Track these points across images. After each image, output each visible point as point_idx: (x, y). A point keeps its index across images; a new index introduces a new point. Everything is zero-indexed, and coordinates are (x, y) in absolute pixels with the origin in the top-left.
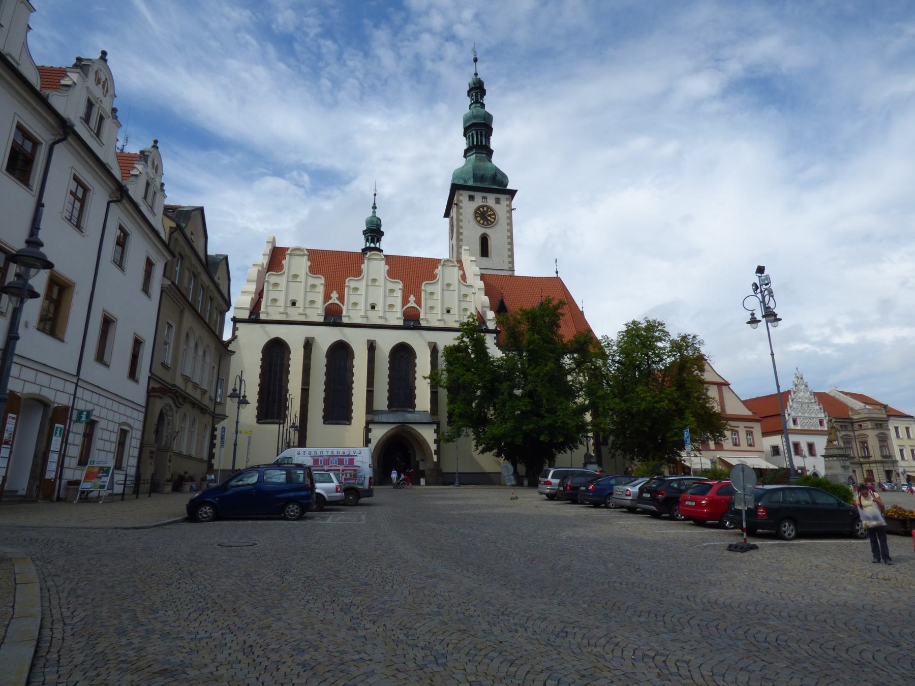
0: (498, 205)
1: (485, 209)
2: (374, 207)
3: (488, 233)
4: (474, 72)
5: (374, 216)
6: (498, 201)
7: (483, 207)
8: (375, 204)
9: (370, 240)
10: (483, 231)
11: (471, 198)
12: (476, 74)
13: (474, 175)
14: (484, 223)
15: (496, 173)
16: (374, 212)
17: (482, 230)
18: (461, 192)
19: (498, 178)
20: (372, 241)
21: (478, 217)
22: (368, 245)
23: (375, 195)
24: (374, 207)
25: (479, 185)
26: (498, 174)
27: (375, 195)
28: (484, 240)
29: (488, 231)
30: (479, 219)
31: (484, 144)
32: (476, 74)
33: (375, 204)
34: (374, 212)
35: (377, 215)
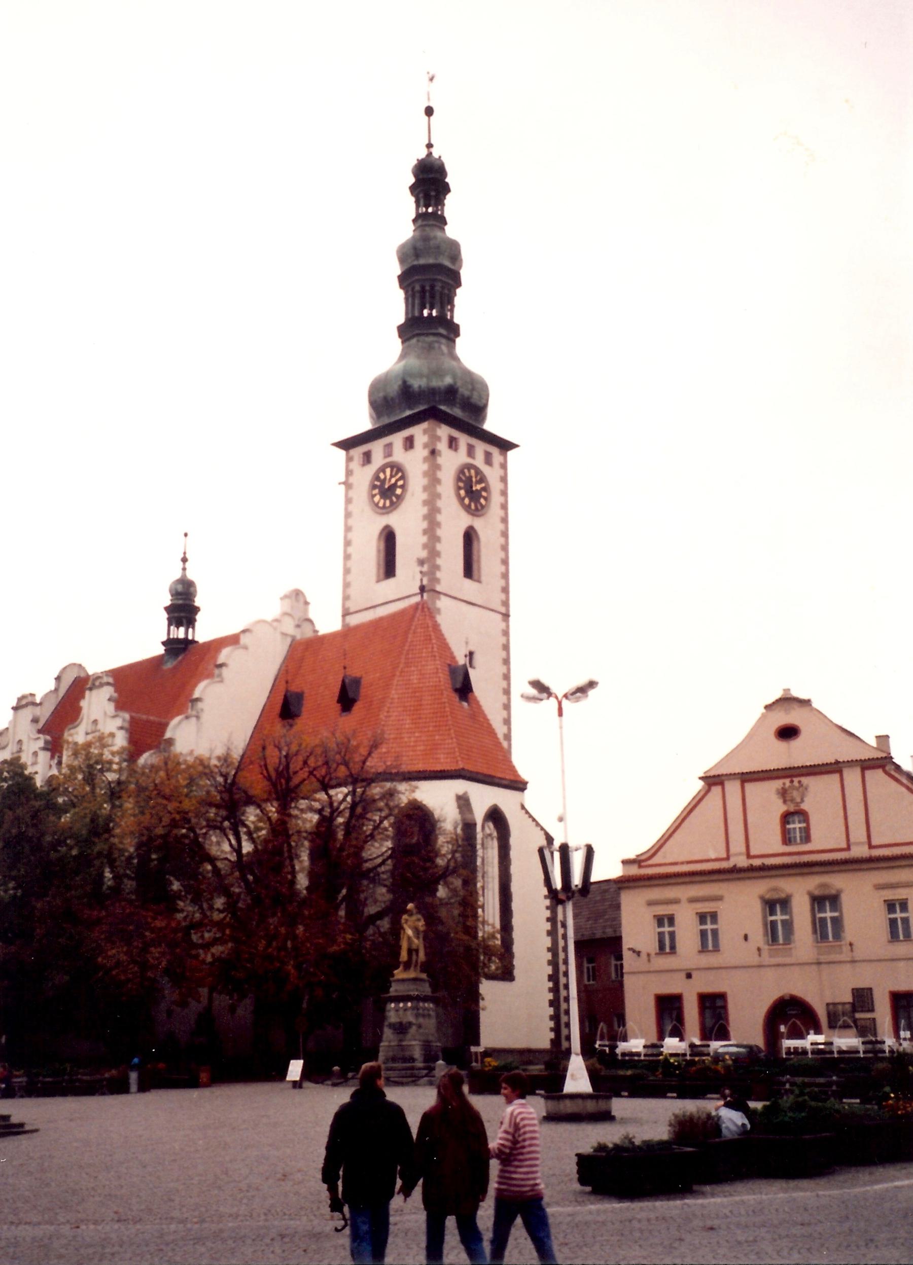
0: (411, 453)
4: (427, 142)
5: (184, 576)
6: (409, 443)
7: (382, 469)
8: (185, 553)
10: (383, 521)
12: (429, 146)
14: (384, 504)
15: (404, 382)
16: (184, 569)
17: (382, 521)
20: (179, 624)
21: (375, 495)
24: (184, 560)
25: (386, 420)
29: (394, 520)
30: (377, 498)
32: (429, 146)
34: (184, 569)
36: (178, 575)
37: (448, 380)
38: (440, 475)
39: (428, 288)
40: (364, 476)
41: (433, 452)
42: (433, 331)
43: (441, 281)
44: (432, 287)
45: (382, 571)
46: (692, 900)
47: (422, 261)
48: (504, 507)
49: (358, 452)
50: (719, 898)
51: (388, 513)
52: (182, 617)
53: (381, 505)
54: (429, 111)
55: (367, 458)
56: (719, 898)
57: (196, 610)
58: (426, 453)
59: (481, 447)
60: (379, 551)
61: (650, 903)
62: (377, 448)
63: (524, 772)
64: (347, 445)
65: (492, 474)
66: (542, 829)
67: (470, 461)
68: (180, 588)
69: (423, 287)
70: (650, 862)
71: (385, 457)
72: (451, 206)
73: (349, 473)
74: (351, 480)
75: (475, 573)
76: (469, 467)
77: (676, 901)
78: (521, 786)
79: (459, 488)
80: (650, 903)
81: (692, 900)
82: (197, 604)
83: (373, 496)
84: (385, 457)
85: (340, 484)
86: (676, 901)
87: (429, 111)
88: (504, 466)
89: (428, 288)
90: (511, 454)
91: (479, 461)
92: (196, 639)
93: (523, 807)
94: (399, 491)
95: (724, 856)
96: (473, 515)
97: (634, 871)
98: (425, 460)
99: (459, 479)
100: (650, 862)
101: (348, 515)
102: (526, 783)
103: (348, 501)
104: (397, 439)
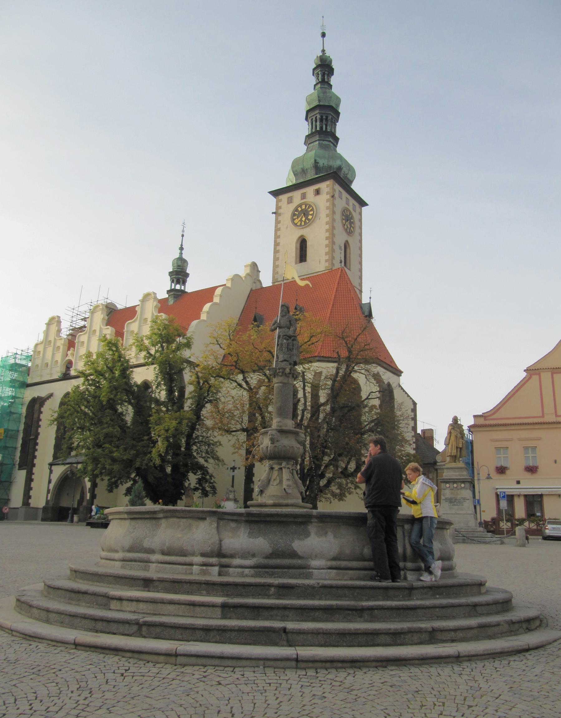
0: (318, 197)
1: (303, 207)
2: (181, 248)
3: (305, 234)
6: (318, 192)
7: (300, 206)
8: (182, 245)
9: (175, 282)
11: (290, 201)
12: (323, 51)
13: (294, 172)
15: (315, 160)
16: (181, 254)
18: (281, 197)
19: (321, 164)
20: (178, 282)
22: (173, 287)
23: (183, 236)
24: (181, 248)
26: (318, 160)
27: (183, 236)
28: (303, 244)
29: (306, 232)
31: (324, 129)
32: (323, 51)
33: (182, 245)
34: (181, 254)
35: (184, 256)
36: (177, 256)
37: (338, 163)
38: (335, 209)
39: (324, 117)
40: (288, 210)
41: (333, 196)
42: (327, 139)
43: (332, 115)
44: (327, 117)
45: (298, 259)
46: (520, 440)
47: (321, 104)
48: (360, 235)
49: (284, 198)
50: (539, 439)
51: (303, 228)
52: (180, 278)
53: (299, 224)
54: (323, 35)
55: (290, 201)
56: (539, 439)
57: (187, 275)
58: (328, 197)
59: (352, 201)
60: (296, 248)
61: (493, 440)
62: (297, 195)
63: (400, 366)
64: (276, 193)
65: (355, 216)
66: (411, 398)
67: (347, 206)
68: (180, 263)
69: (322, 117)
70: (490, 418)
71: (302, 199)
72: (333, 80)
73: (278, 207)
74: (280, 211)
75: (348, 265)
76: (348, 210)
77: (511, 440)
78: (399, 374)
79: (343, 219)
80: (493, 440)
81: (520, 440)
82: (187, 272)
83: (294, 220)
84: (302, 199)
85: (273, 213)
86: (511, 440)
87: (323, 35)
88: (360, 214)
89: (324, 117)
90: (364, 209)
91: (351, 208)
92: (186, 290)
93: (400, 386)
94: (310, 217)
95: (541, 415)
96: (348, 235)
97: (481, 421)
98: (328, 201)
99: (343, 215)
100: (490, 418)
101: (277, 230)
102: (401, 372)
103: (277, 222)
104: (310, 191)
